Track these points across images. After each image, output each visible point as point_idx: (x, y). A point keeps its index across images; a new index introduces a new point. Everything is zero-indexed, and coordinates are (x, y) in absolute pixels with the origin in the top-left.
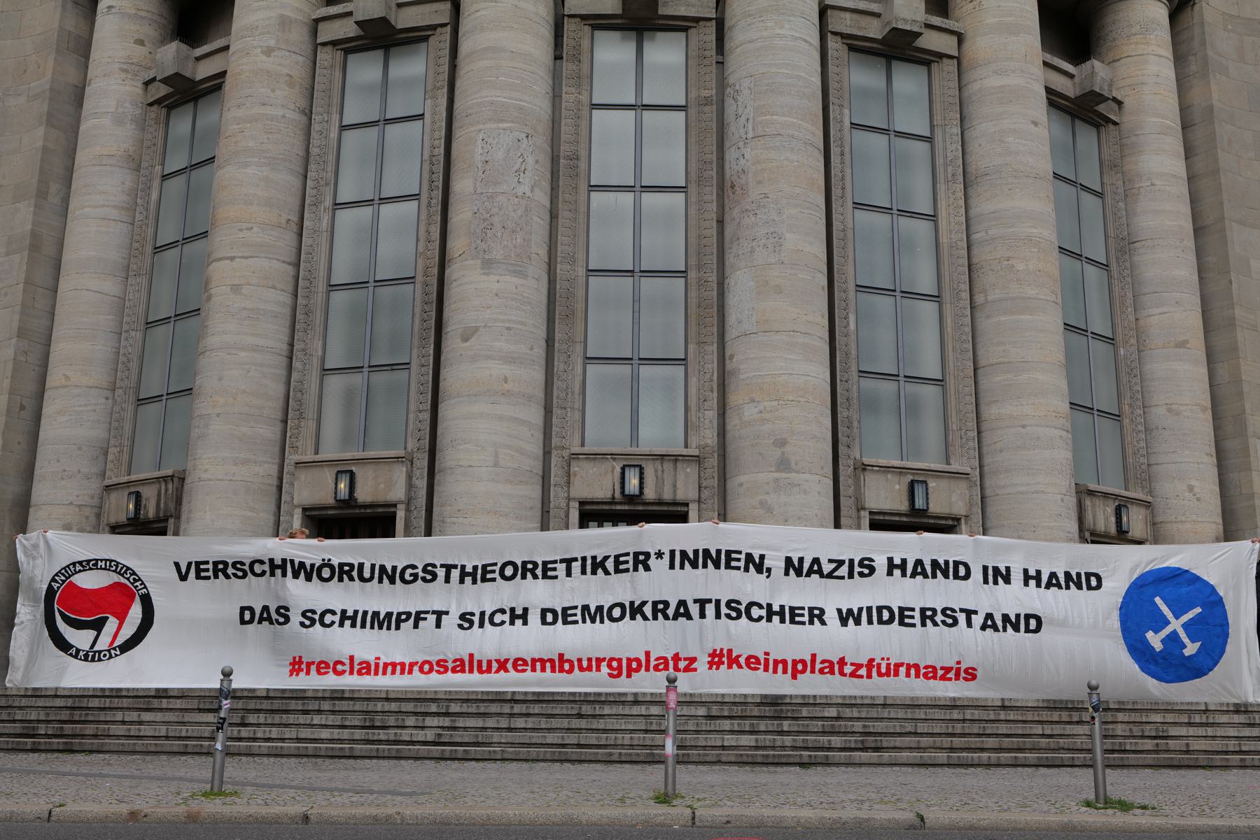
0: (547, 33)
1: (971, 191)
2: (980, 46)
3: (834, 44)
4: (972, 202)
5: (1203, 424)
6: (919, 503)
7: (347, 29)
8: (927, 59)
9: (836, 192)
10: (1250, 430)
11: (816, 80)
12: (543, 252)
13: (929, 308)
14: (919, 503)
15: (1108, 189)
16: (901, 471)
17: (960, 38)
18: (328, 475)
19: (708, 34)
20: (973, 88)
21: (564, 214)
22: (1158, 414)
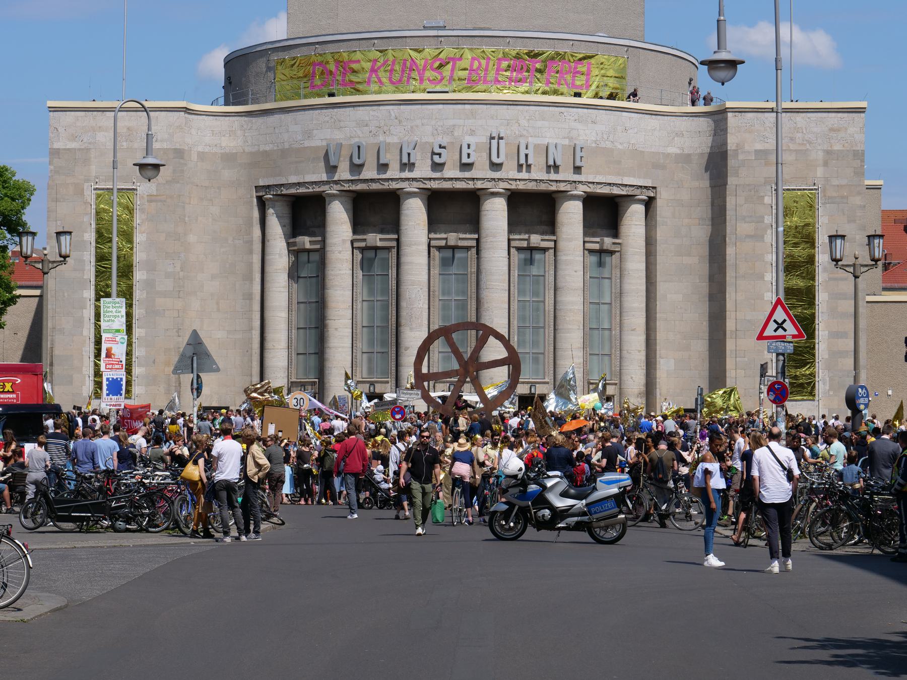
0: (426, 254)
1: (558, 292)
2: (562, 245)
3: (512, 250)
4: (558, 296)
5: (642, 356)
6: (533, 391)
7: (363, 244)
8: (544, 250)
9: (512, 299)
10: (658, 356)
11: (506, 268)
12: (426, 323)
13: (542, 330)
14: (533, 391)
15: (614, 275)
16: (528, 383)
17: (555, 241)
18: (368, 385)
19: (474, 251)
20: (559, 258)
21: (431, 309)
22: (624, 352)
